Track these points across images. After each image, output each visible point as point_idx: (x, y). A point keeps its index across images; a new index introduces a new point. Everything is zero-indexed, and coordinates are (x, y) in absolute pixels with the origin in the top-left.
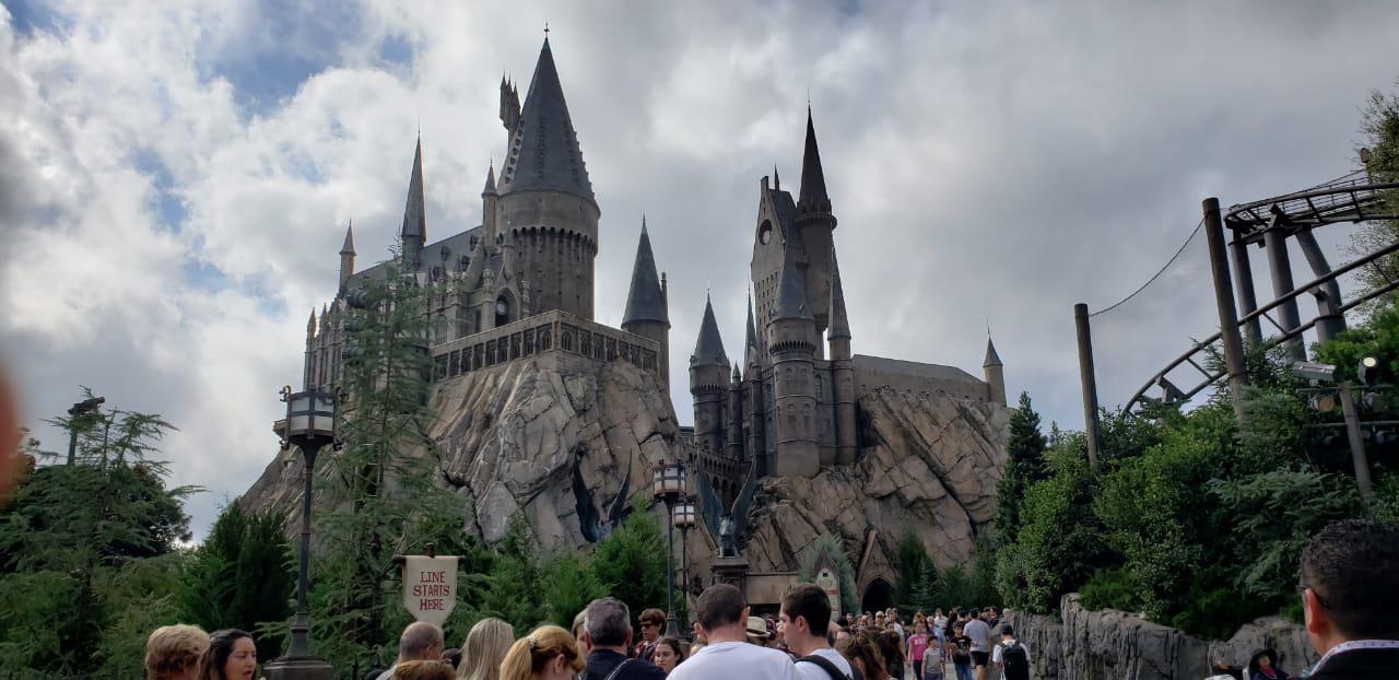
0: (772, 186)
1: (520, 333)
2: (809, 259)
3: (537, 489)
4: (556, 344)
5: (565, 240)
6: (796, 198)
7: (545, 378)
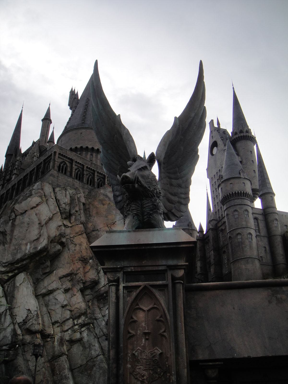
0: (216, 125)
1: (35, 168)
2: (242, 158)
3: (18, 268)
4: (53, 167)
5: (94, 154)
6: (230, 131)
7: (40, 187)
